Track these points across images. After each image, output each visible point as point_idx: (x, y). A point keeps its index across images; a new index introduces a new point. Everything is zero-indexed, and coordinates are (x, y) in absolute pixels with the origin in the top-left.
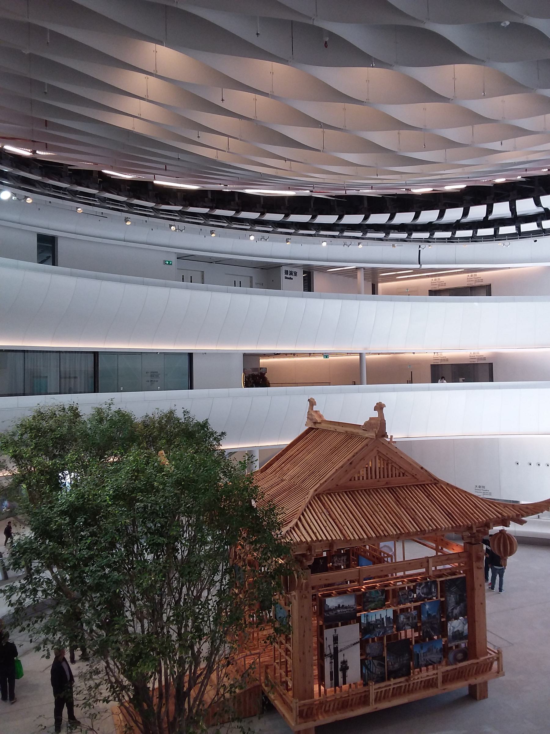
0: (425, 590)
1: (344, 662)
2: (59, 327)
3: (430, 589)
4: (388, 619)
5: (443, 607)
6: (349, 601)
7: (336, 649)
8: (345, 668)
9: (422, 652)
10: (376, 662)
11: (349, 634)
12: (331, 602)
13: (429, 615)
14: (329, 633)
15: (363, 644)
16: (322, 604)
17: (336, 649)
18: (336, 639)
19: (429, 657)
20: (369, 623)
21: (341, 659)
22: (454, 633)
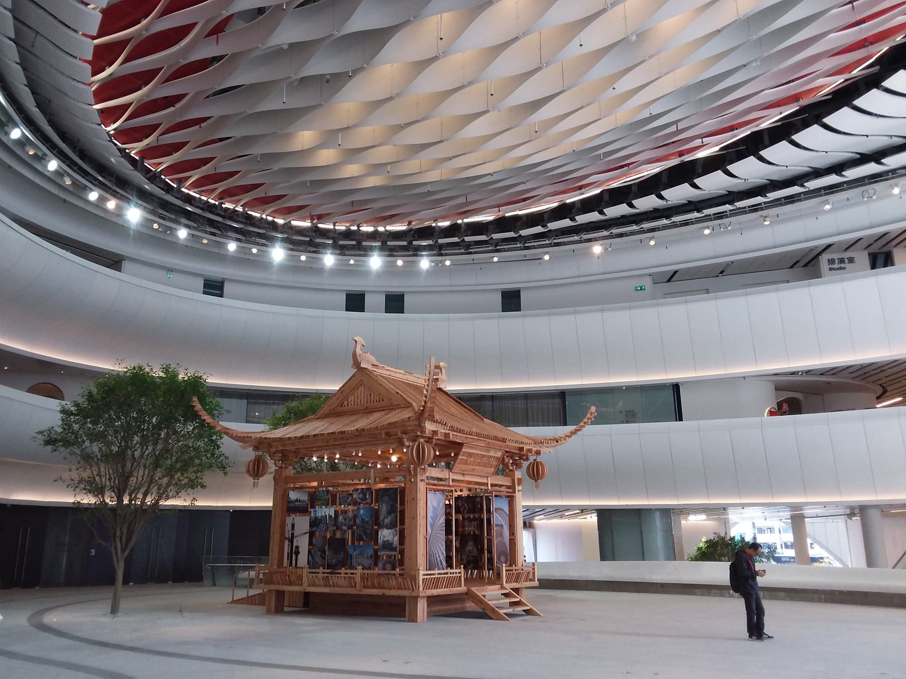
0: (361, 496)
1: (297, 547)
2: (502, 367)
3: (365, 495)
4: (330, 516)
5: (376, 514)
6: (304, 497)
7: (293, 534)
8: (297, 553)
9: (355, 553)
10: (319, 553)
11: (302, 523)
12: (293, 495)
13: (363, 519)
14: (289, 521)
15: (312, 535)
16: (285, 495)
17: (293, 534)
18: (293, 526)
19: (360, 561)
20: (316, 518)
21: (295, 544)
22: (384, 542)
